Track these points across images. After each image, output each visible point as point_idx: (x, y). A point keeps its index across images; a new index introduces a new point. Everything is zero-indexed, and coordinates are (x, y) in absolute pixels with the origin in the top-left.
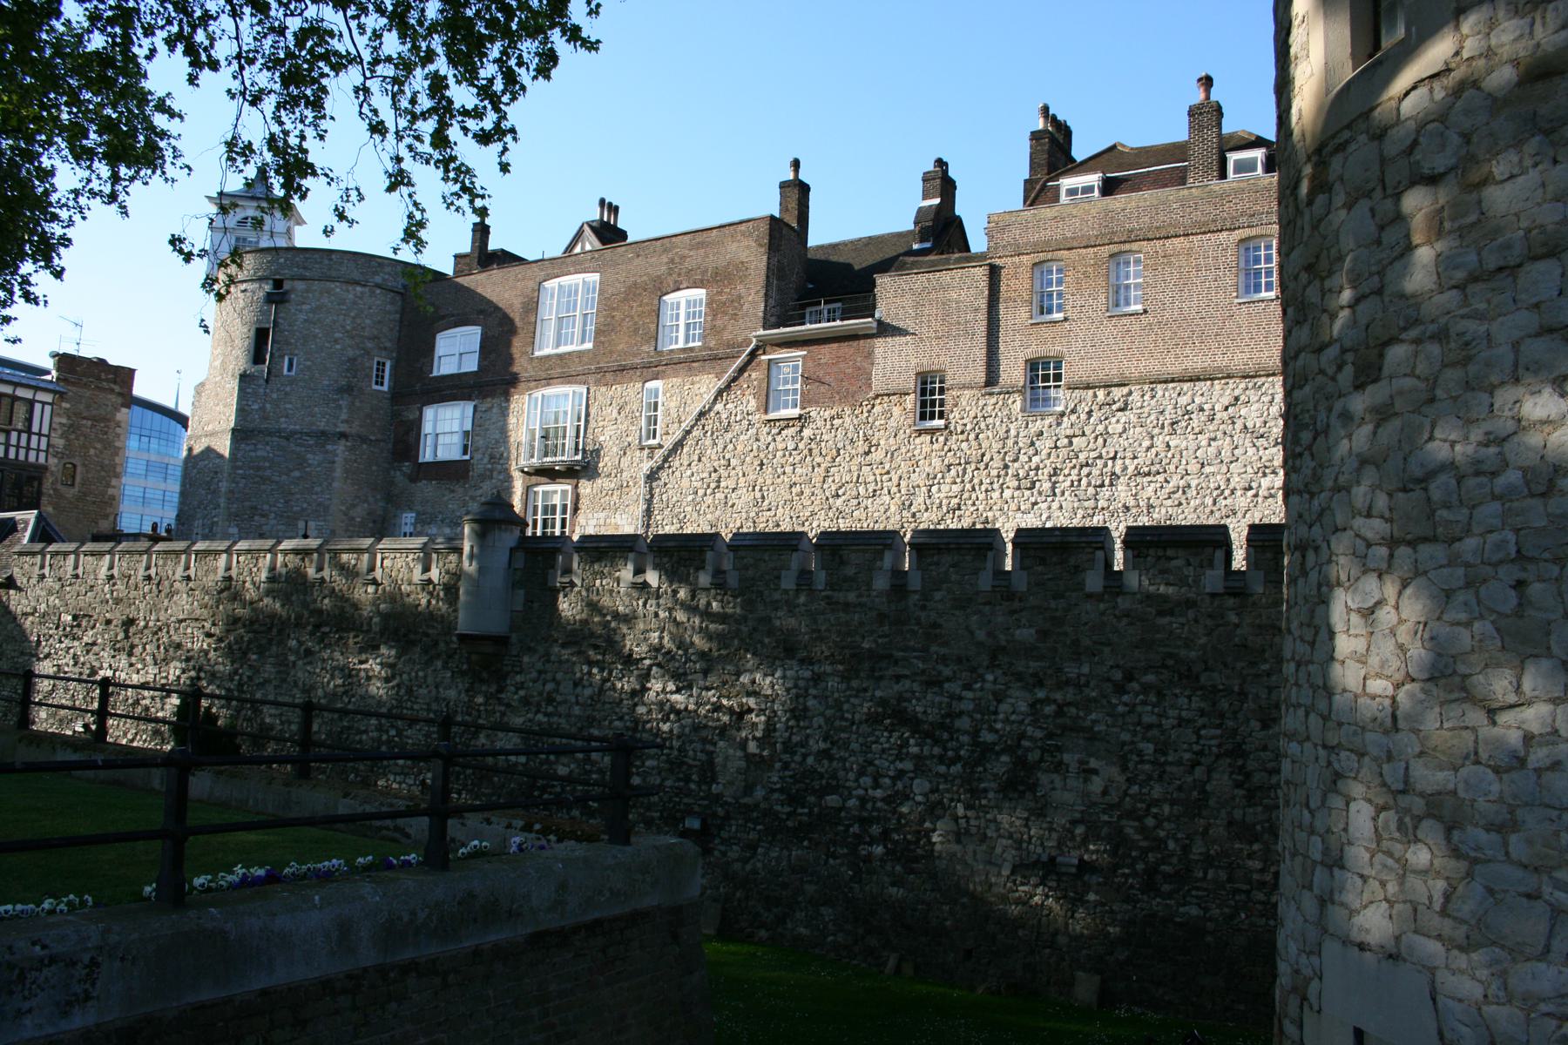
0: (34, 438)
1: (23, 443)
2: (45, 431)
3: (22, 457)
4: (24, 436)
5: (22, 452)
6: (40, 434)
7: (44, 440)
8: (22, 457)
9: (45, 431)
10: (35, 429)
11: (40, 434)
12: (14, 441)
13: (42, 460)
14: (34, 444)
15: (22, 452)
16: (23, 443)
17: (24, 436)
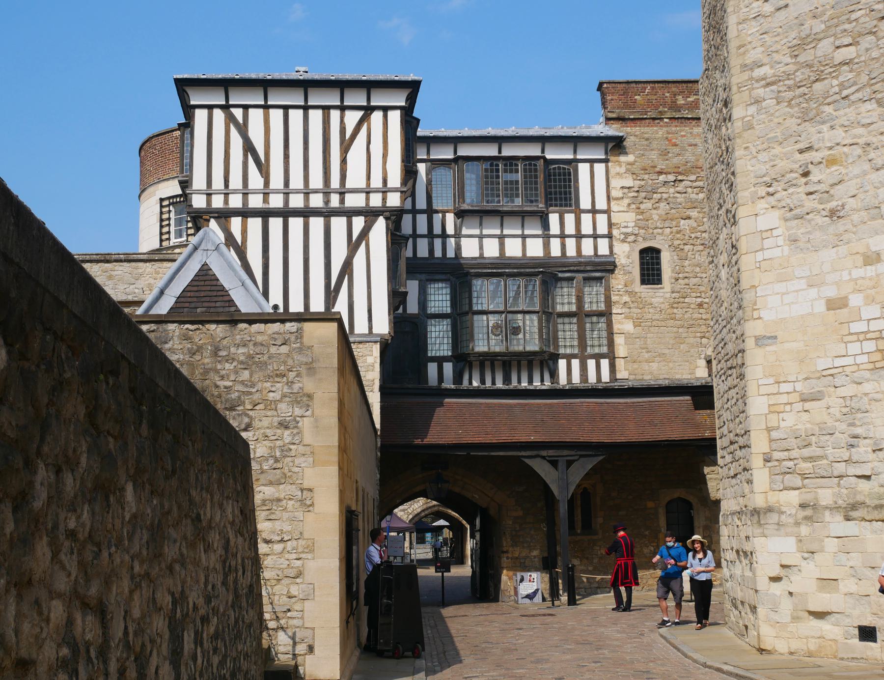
0: (586, 219)
1: (570, 229)
2: (601, 204)
3: (571, 252)
4: (570, 218)
5: (571, 243)
6: (594, 211)
7: (602, 219)
8: (571, 252)
9: (601, 204)
10: (585, 202)
11: (594, 211)
12: (555, 228)
13: (603, 247)
14: (587, 229)
15: (571, 243)
16: (570, 229)
17: (570, 218)
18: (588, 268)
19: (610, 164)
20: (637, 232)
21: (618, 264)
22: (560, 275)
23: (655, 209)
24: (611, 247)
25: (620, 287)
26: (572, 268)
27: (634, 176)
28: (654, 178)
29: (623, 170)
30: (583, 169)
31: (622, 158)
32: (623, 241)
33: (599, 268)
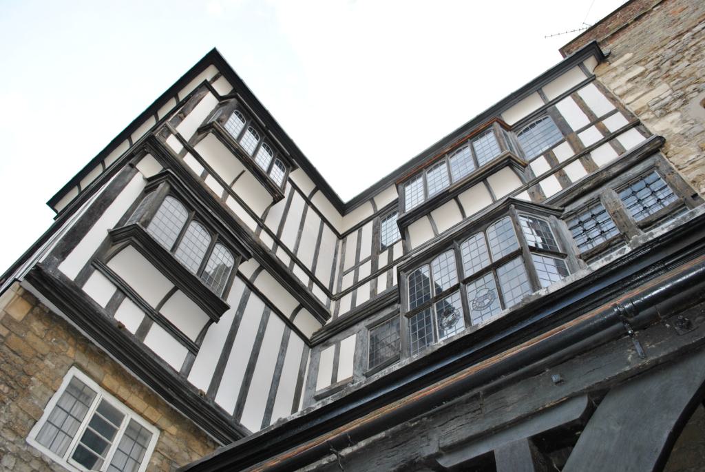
13: (633, 140)
18: (615, 170)
19: (599, 79)
20: (682, 93)
21: (667, 139)
22: (568, 209)
23: (694, 62)
24: (646, 133)
25: (691, 157)
26: (585, 187)
27: (643, 63)
28: (672, 44)
29: (621, 69)
30: (567, 109)
31: (614, 65)
32: (662, 116)
33: (634, 159)
